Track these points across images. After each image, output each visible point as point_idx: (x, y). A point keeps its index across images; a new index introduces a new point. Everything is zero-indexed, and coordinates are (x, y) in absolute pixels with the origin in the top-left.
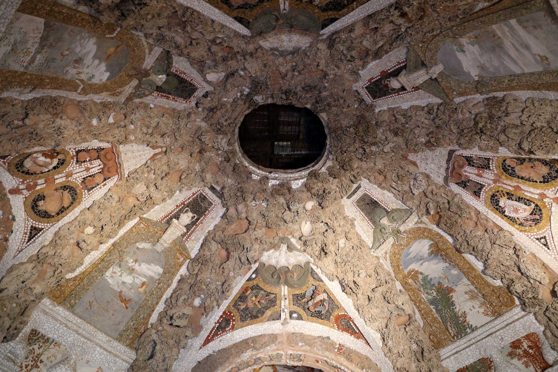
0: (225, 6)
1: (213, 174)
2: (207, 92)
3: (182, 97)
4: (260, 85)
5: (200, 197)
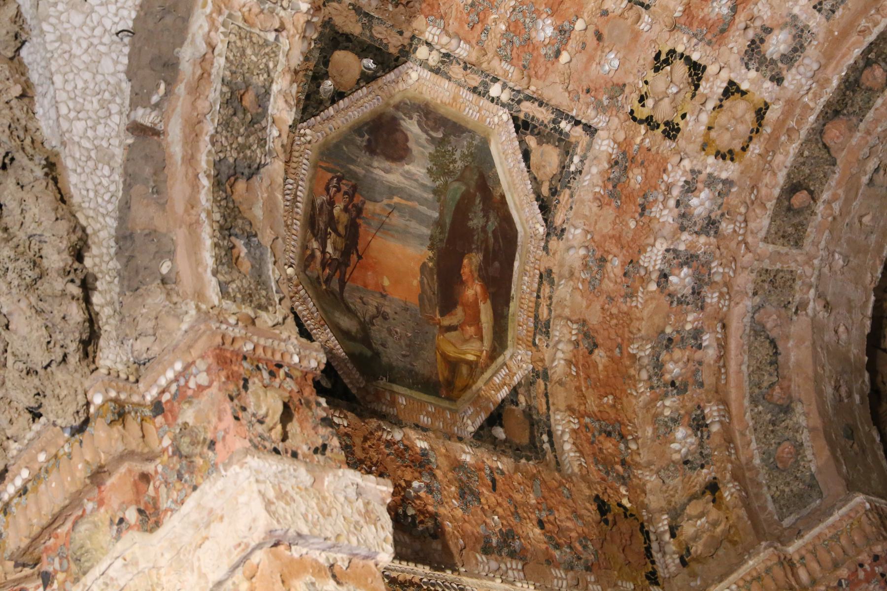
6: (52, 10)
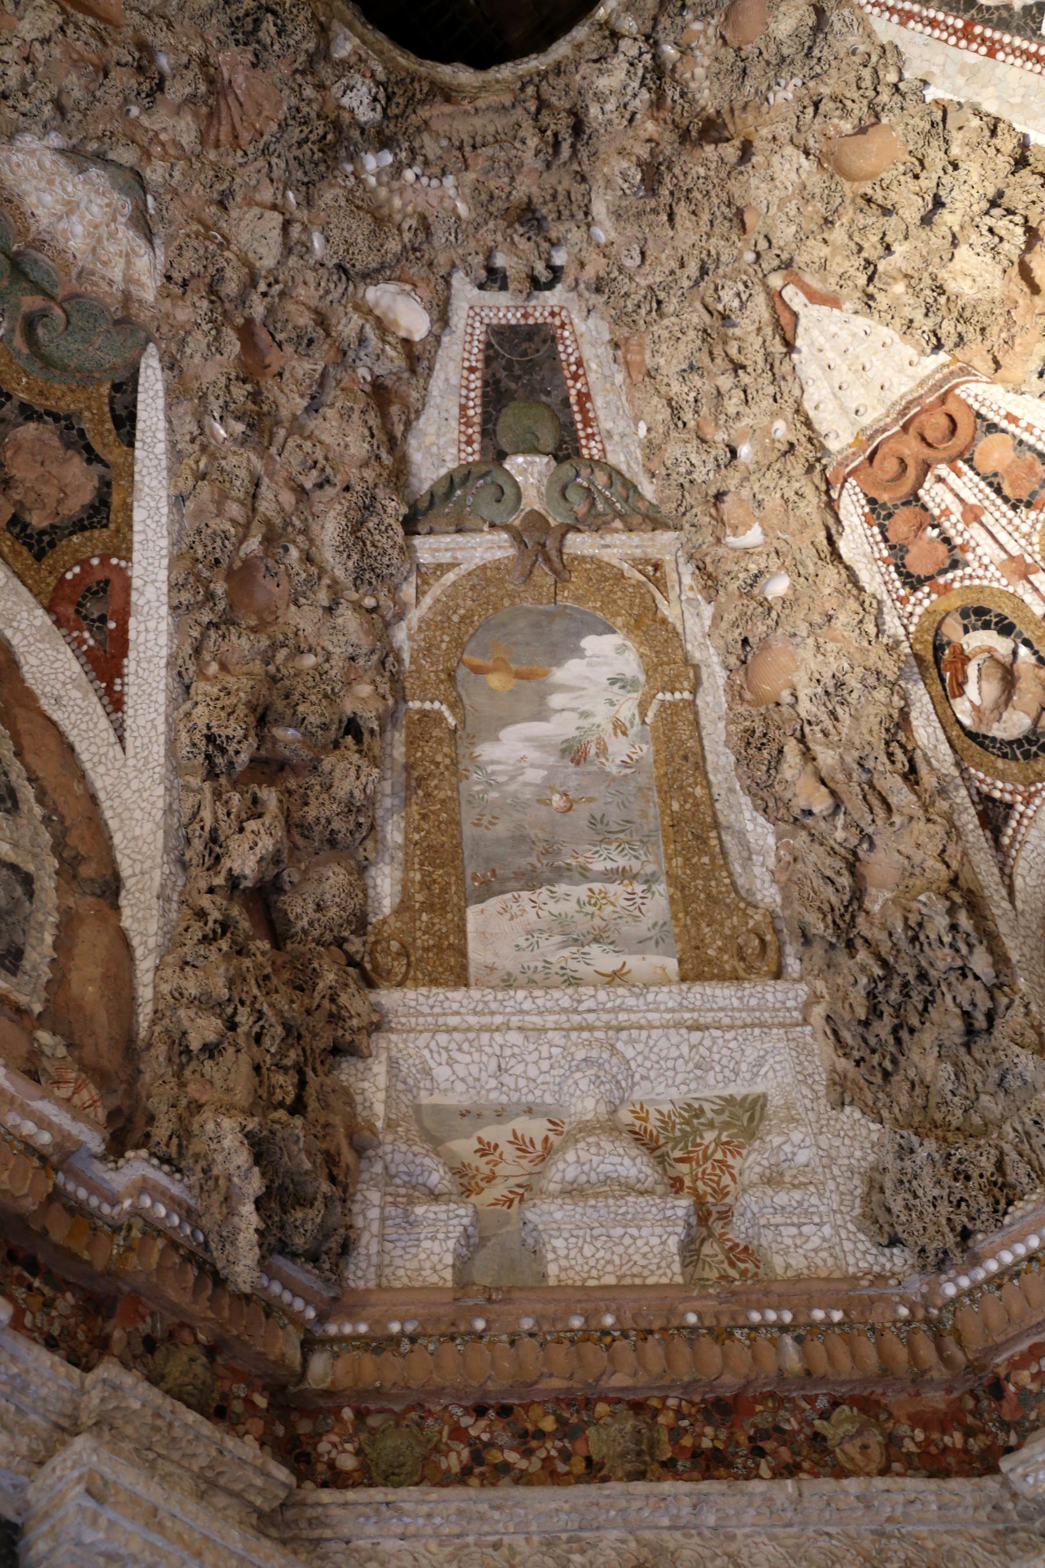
0: (116, 500)
2: (481, 287)
3: (554, 355)
4: (299, 153)
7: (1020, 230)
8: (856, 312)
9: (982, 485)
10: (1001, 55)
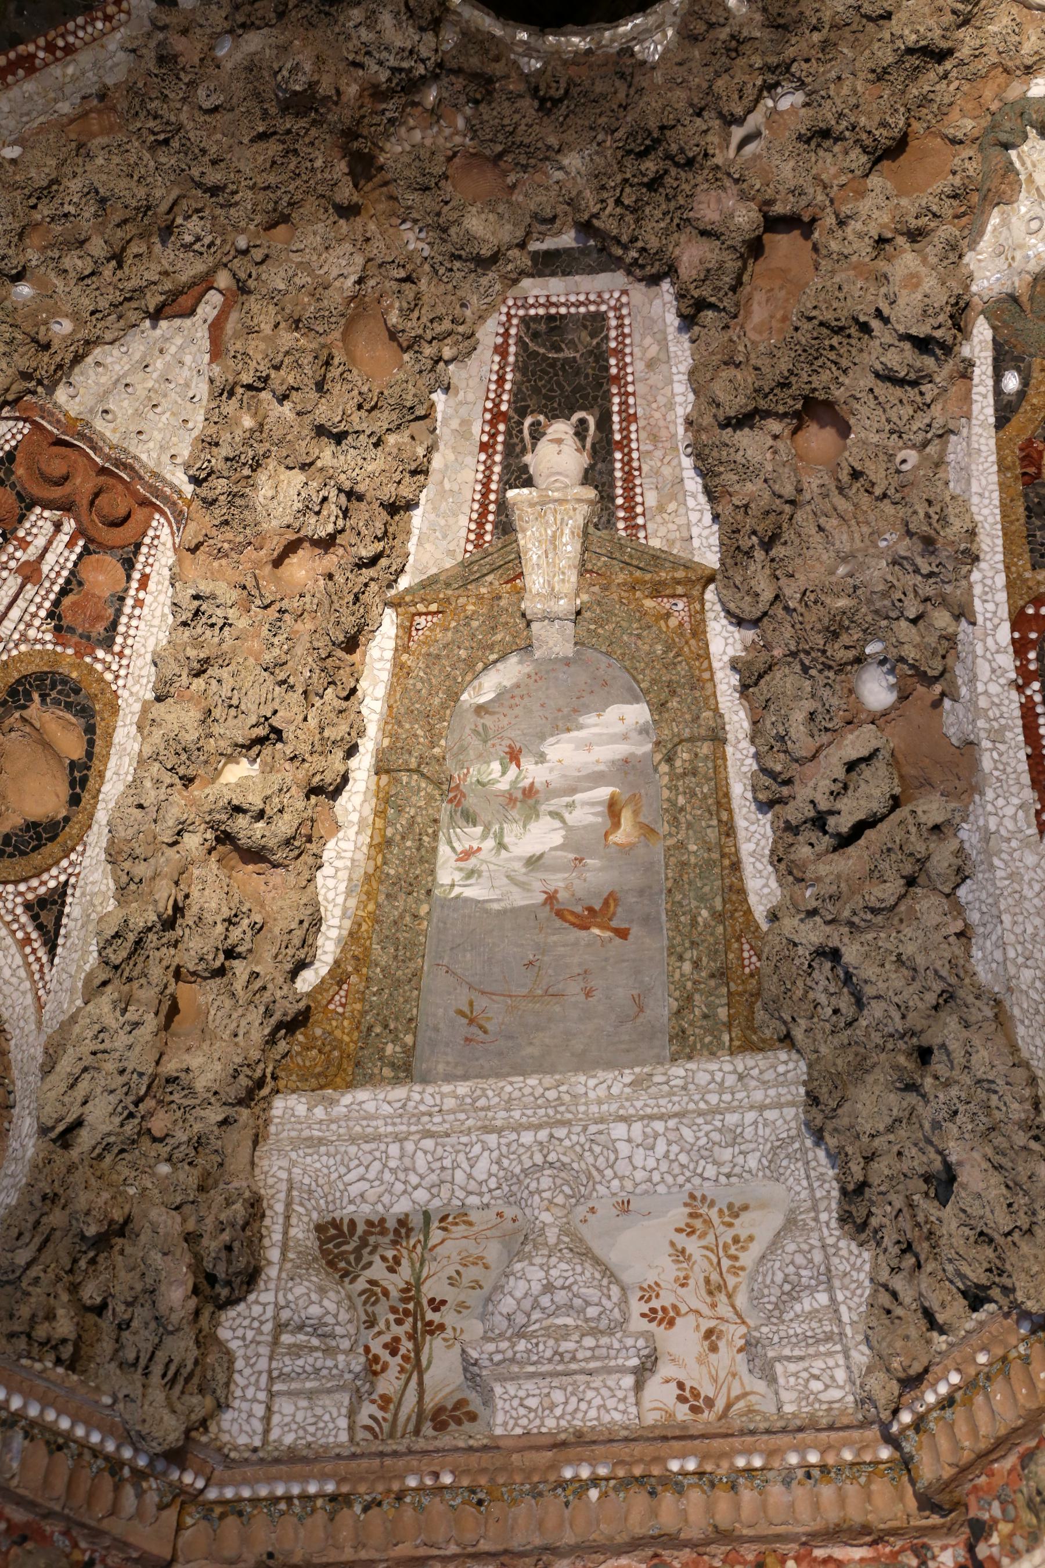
1: (491, 205)
5: (535, 336)
6: (1004, 846)
7: (330, 528)
8: (211, 381)
9: (65, 573)
10: (483, 457)
